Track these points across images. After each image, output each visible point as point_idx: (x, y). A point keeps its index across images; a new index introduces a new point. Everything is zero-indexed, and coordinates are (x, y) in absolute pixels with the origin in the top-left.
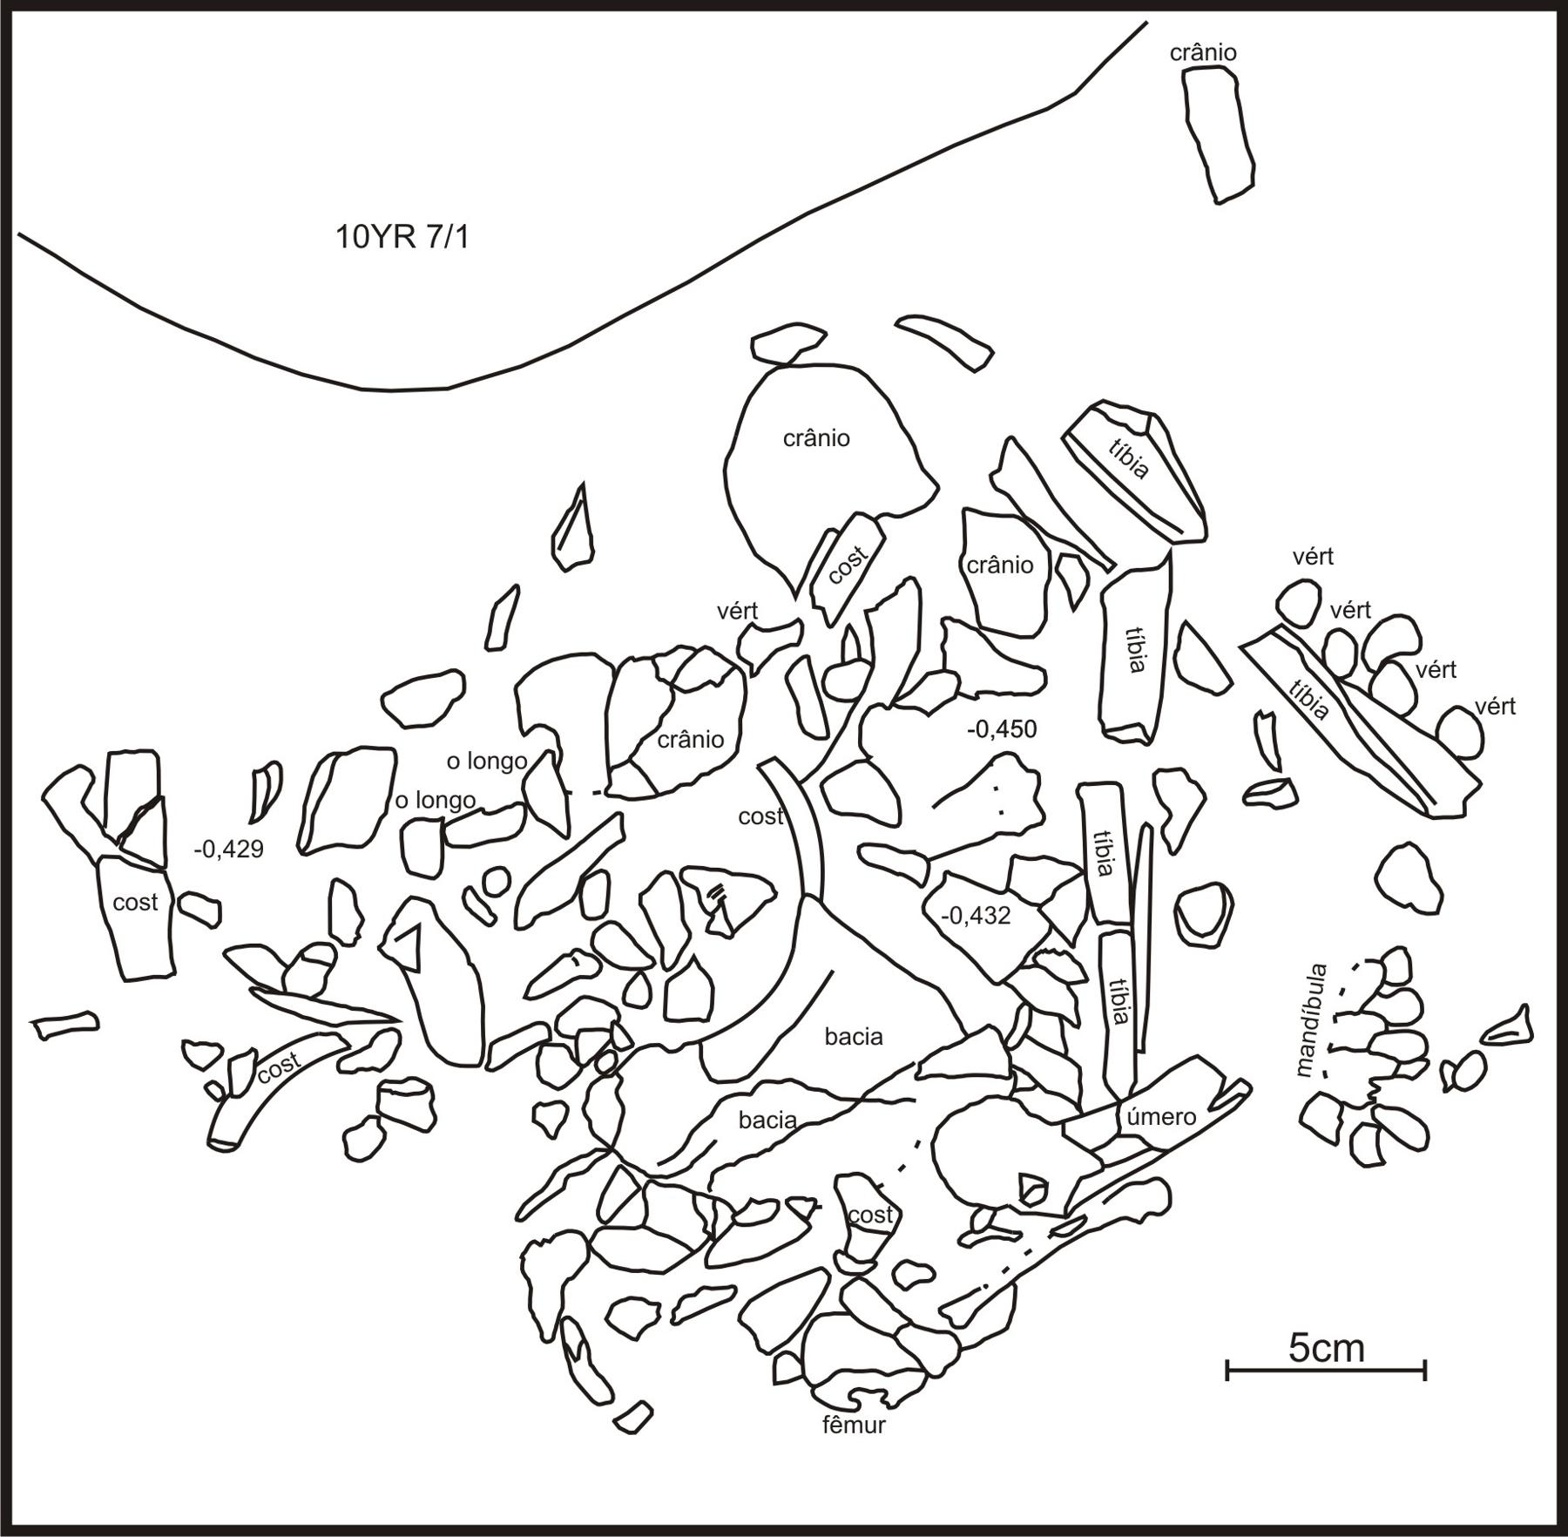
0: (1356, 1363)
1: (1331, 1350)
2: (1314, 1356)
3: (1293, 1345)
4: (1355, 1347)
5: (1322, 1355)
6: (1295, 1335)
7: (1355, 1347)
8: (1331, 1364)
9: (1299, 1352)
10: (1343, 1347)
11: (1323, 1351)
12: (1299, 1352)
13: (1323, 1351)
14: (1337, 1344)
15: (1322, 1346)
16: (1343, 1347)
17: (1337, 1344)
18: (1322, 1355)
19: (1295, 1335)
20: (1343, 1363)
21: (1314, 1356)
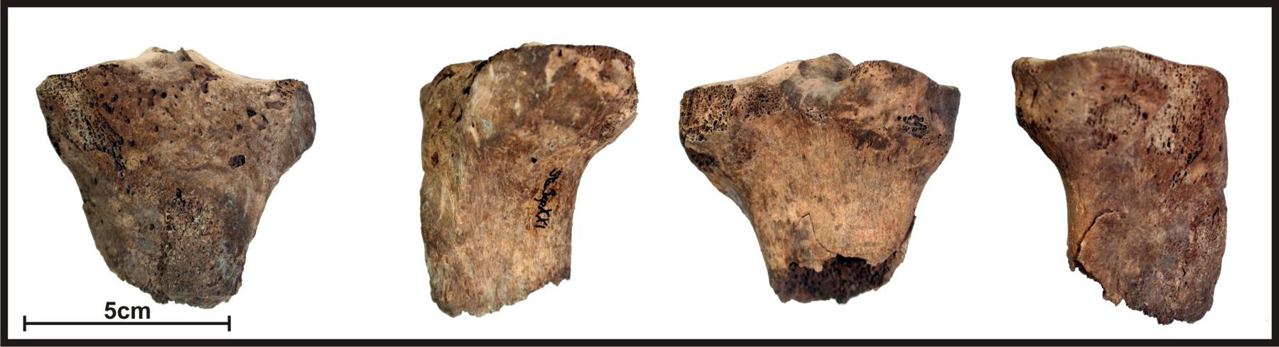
0: (144, 319)
1: (130, 312)
3: (107, 309)
4: (145, 311)
6: (108, 304)
7: (145, 311)
8: (129, 320)
9: (110, 313)
10: (137, 311)
11: (124, 313)
12: (110, 313)
13: (124, 313)
16: (137, 311)
17: (134, 309)
19: (108, 304)
20: (137, 319)
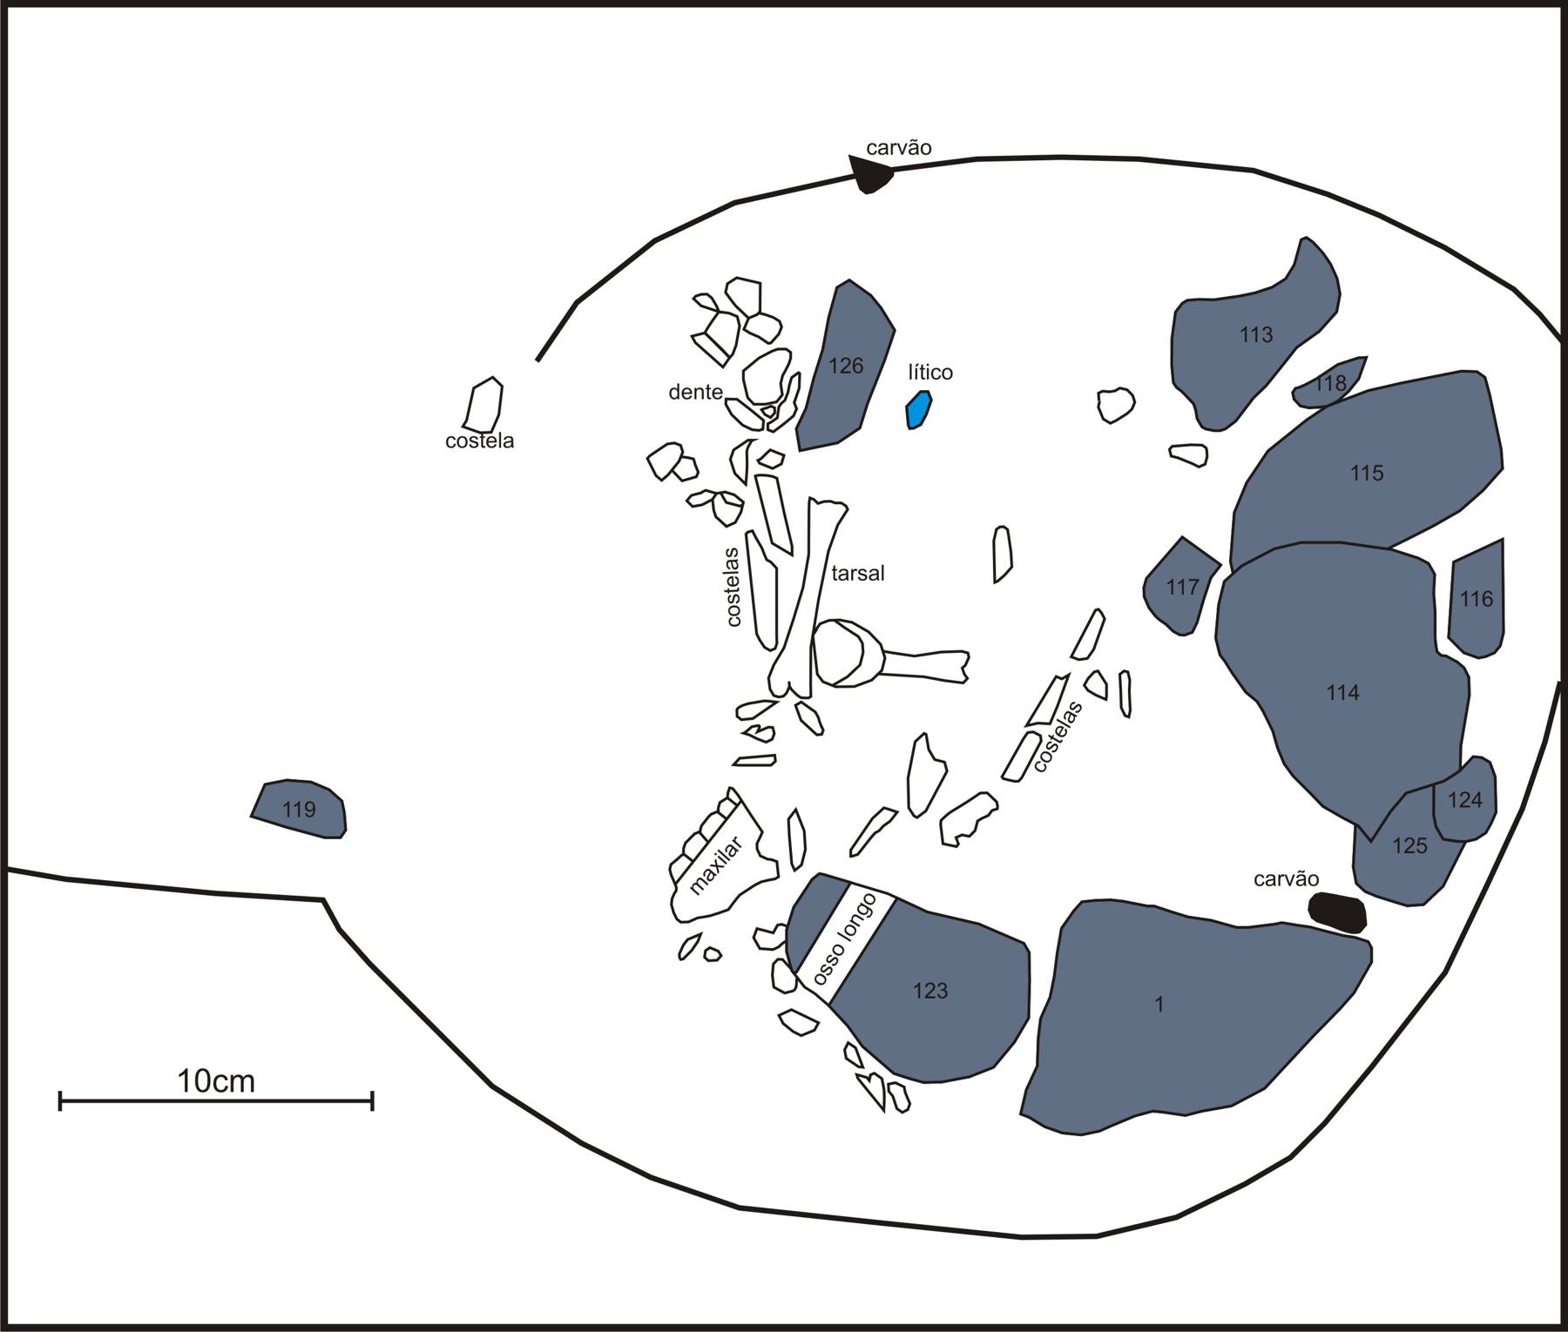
0: (247, 1095)
1: (228, 1083)
2: (213, 1088)
4: (247, 1081)
5: (221, 1087)
7: (247, 1081)
10: (237, 1081)
11: (221, 1083)
13: (221, 1083)
14: (233, 1078)
15: (220, 1080)
16: (237, 1081)
17: (233, 1078)
18: (221, 1087)
20: (237, 1095)
21: (213, 1088)
